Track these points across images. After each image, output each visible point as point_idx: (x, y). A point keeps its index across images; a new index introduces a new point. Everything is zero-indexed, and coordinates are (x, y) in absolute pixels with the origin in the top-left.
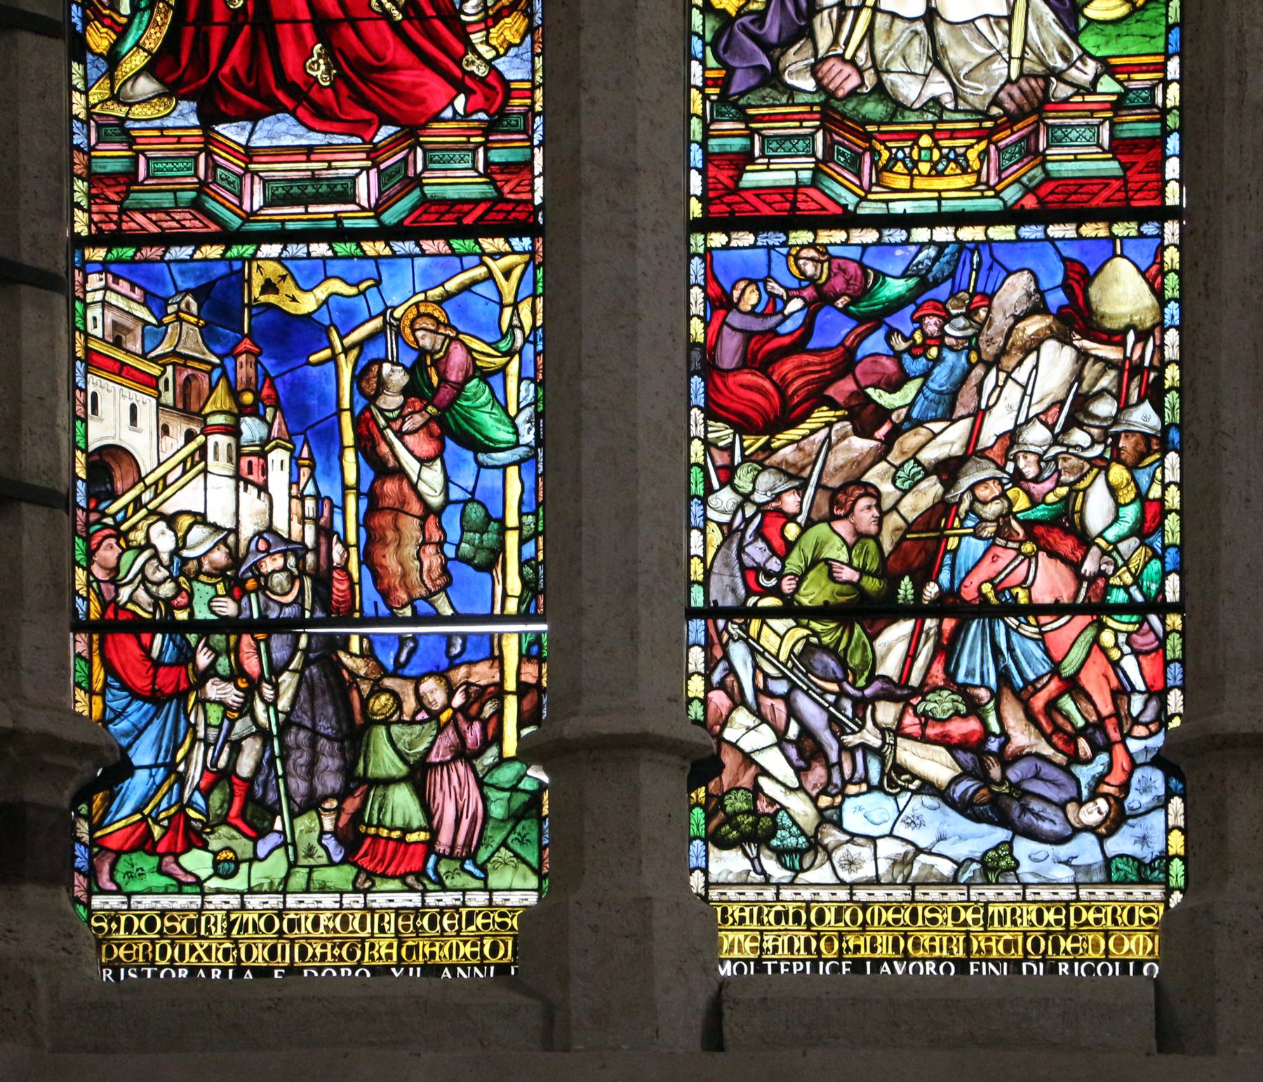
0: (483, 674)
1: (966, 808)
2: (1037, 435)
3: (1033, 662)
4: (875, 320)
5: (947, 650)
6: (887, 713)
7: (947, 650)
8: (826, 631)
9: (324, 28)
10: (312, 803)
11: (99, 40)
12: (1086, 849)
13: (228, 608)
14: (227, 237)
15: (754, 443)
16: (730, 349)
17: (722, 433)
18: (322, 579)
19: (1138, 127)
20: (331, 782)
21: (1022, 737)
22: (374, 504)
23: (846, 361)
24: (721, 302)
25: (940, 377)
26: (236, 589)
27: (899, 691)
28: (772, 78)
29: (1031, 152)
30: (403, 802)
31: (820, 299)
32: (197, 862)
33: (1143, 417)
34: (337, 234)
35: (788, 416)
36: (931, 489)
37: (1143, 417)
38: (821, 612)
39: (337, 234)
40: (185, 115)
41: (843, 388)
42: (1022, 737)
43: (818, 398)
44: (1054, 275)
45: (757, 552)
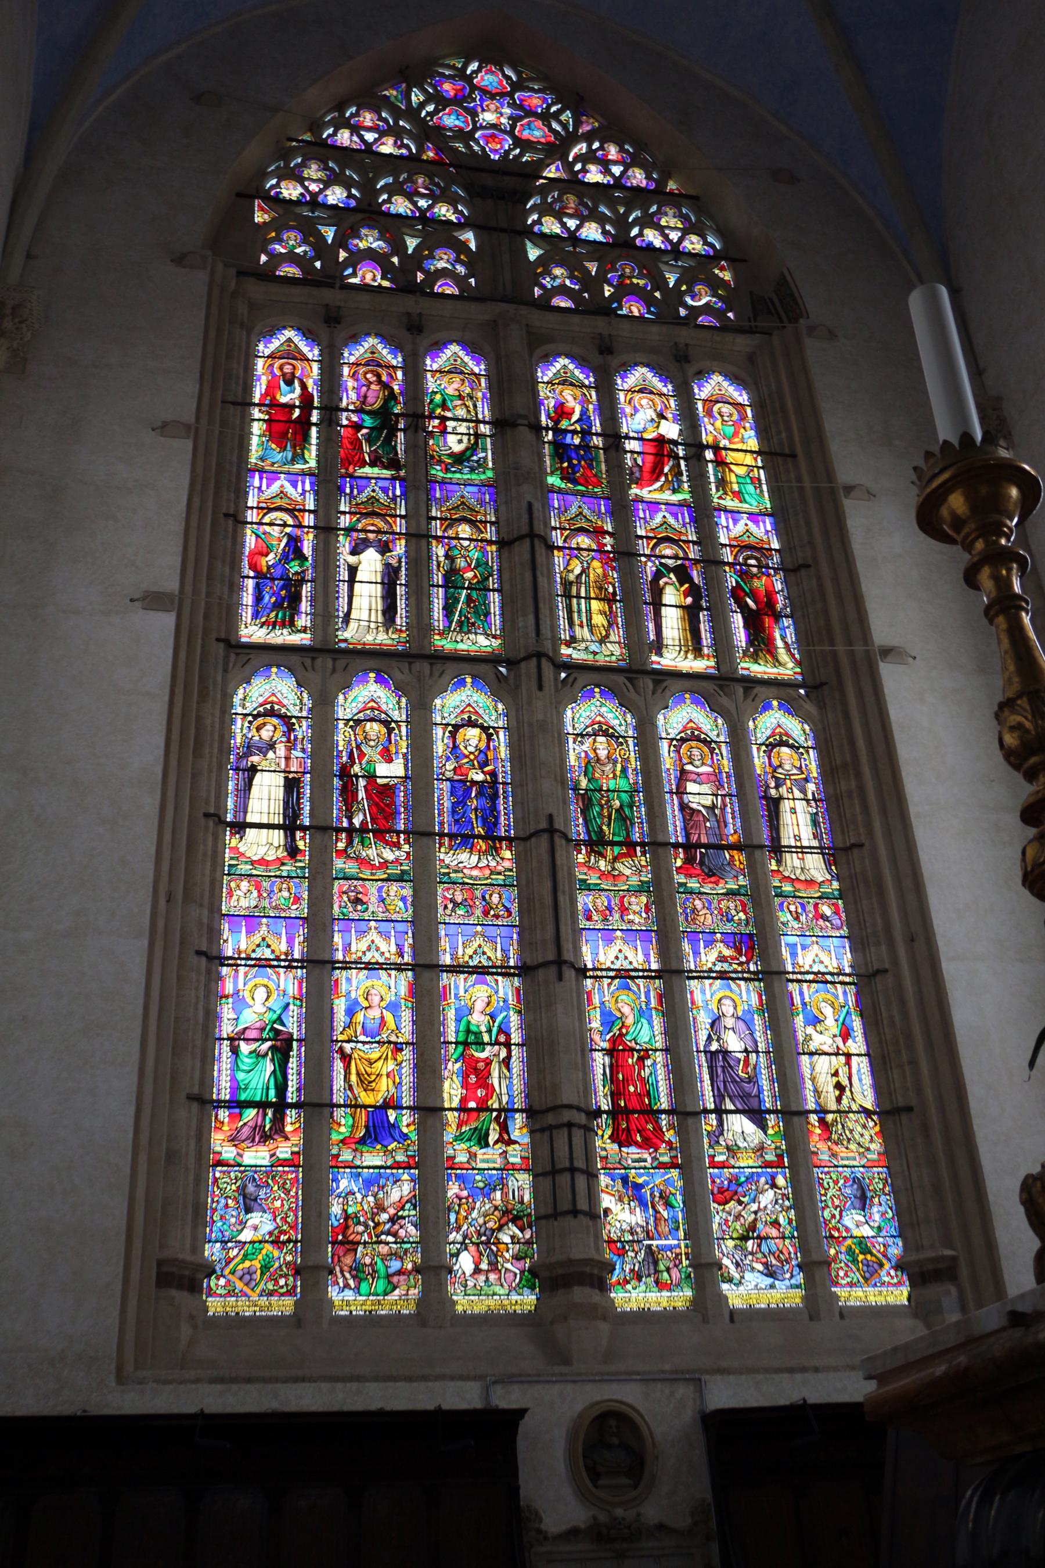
0: (678, 1251)
1: (766, 1275)
2: (770, 1206)
3: (774, 1248)
4: (740, 1185)
5: (759, 1246)
6: (750, 1257)
7: (759, 1246)
8: (738, 1242)
9: (639, 1131)
10: (649, 1275)
11: (600, 1132)
12: (787, 1282)
13: (631, 1238)
14: (625, 1168)
15: (722, 1207)
16: (716, 1191)
17: (716, 1205)
18: (648, 1233)
19: (779, 1152)
20: (652, 1271)
21: (774, 1262)
22: (656, 1219)
23: (736, 1193)
24: (713, 1182)
25: (752, 1196)
26: (632, 1234)
27: (752, 1253)
28: (718, 1142)
29: (762, 1156)
30: (665, 1275)
31: (730, 1181)
32: (629, 1287)
33: (787, 1203)
34: (645, 1168)
35: (726, 1202)
36: (753, 1216)
37: (787, 1203)
38: (737, 1239)
39: (645, 1168)
40: (616, 1146)
41: (736, 1197)
42: (774, 1262)
43: (731, 1199)
44: (769, 1178)
45: (724, 1227)
